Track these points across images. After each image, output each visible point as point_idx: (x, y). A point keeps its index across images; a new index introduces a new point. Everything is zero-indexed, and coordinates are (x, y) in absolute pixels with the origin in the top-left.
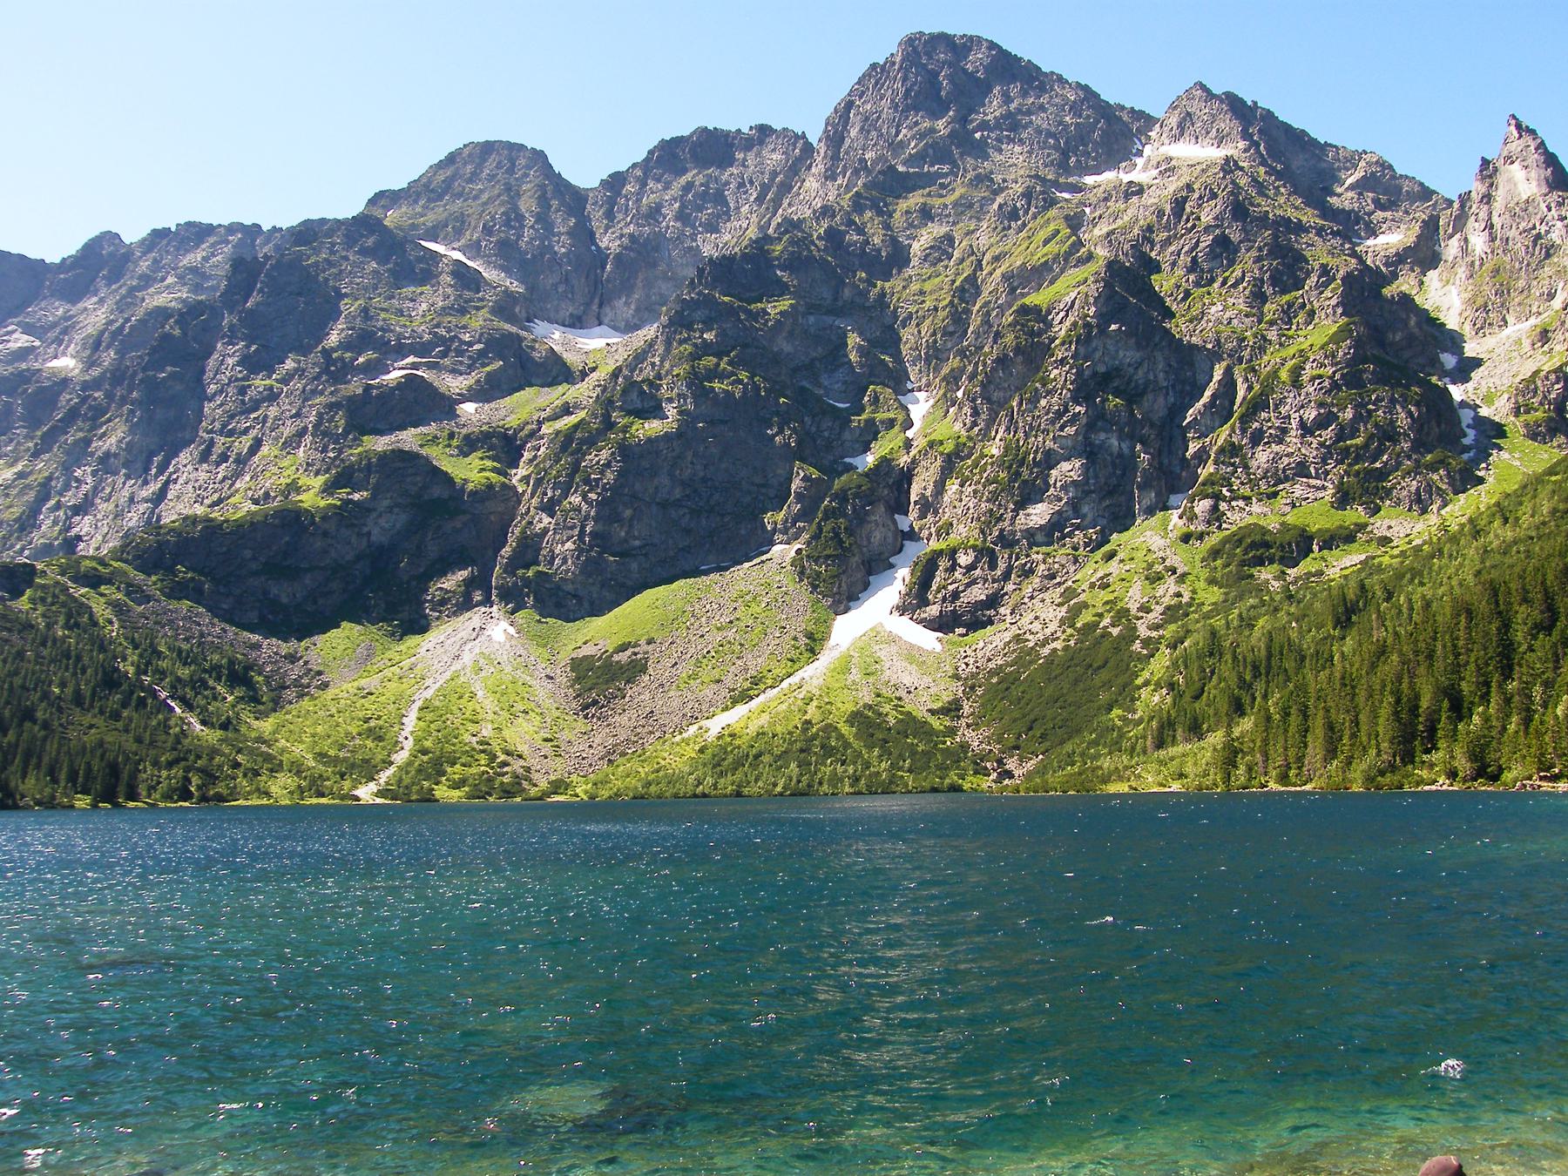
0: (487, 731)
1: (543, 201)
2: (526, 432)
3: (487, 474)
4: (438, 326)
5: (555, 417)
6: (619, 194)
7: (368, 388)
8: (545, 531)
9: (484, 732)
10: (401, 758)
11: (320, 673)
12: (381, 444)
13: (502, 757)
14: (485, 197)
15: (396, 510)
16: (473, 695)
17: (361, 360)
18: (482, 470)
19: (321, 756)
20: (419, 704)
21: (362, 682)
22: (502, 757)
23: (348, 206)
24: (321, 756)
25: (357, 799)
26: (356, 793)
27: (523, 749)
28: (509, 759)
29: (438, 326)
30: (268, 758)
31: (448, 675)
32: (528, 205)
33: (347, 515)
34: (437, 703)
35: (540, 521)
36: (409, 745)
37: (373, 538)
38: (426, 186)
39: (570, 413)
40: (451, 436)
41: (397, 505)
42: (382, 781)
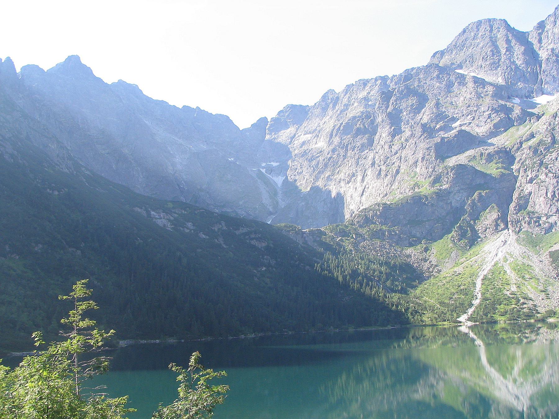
0: (514, 288)
1: (508, 41)
2: (515, 148)
3: (500, 170)
4: (469, 106)
5: (528, 140)
6: (543, 31)
7: (443, 139)
8: (530, 193)
9: (513, 289)
10: (476, 302)
11: (436, 266)
12: (452, 161)
13: (522, 301)
14: (481, 45)
15: (461, 191)
16: (505, 272)
17: (438, 126)
18: (497, 169)
19: (442, 303)
20: (482, 277)
21: (456, 269)
22: (522, 301)
23: (423, 61)
24: (442, 303)
25: (460, 322)
26: (458, 319)
27: (531, 296)
28: (525, 301)
29: (469, 106)
30: (419, 305)
31: (493, 263)
32: (502, 46)
33: (440, 195)
34: (490, 277)
35: (527, 189)
36: (479, 296)
37: (453, 205)
38: (455, 46)
39: (533, 137)
40: (482, 154)
41: (462, 189)
42: (469, 314)
